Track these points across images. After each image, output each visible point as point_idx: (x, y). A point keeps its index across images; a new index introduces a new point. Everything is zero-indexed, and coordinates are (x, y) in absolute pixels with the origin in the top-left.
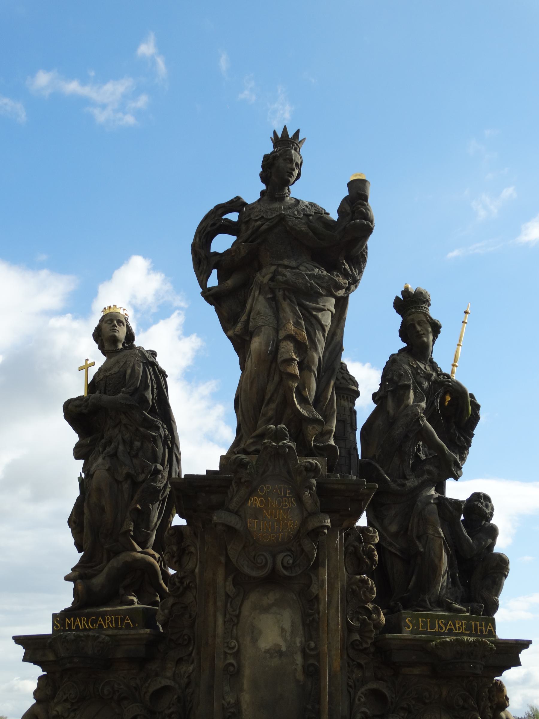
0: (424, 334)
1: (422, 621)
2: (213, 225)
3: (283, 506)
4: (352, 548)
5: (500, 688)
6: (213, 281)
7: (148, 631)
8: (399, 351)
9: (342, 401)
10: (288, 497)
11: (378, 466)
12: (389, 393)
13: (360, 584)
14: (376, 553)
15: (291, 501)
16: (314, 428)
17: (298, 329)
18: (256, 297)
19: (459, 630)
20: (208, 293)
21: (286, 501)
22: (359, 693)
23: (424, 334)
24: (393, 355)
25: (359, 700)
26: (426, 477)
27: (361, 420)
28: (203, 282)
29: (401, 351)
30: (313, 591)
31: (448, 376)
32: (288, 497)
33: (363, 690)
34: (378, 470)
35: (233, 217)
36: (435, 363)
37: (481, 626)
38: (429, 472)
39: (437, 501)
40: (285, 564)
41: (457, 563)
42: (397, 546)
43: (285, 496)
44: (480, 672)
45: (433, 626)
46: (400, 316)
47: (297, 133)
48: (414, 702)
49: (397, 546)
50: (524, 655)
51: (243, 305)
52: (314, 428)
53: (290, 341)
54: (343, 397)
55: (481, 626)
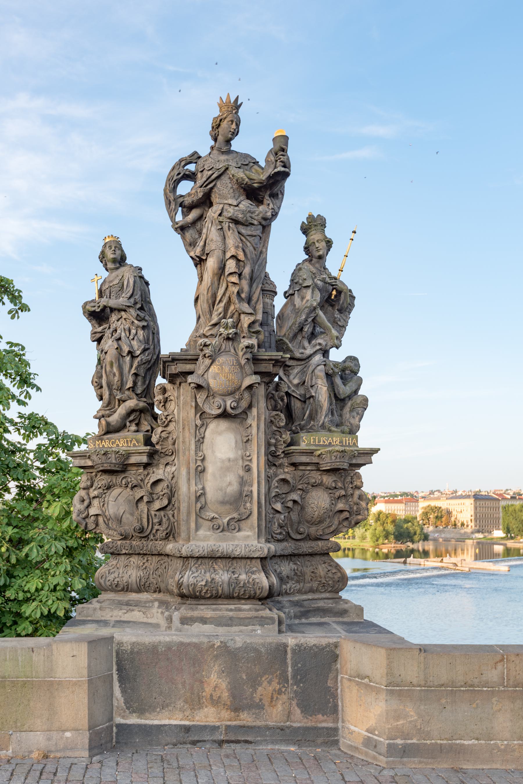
1: (313, 438)
2: (179, 174)
4: (271, 395)
5: (359, 477)
6: (179, 217)
7: (149, 447)
8: (303, 261)
11: (287, 342)
12: (296, 292)
14: (285, 398)
18: (209, 228)
19: (335, 442)
20: (177, 226)
22: (274, 481)
24: (299, 264)
25: (274, 485)
26: (318, 347)
27: (277, 312)
28: (172, 219)
29: (306, 260)
30: (249, 422)
31: (335, 278)
33: (277, 479)
34: (287, 344)
35: (192, 167)
36: (327, 269)
37: (349, 440)
38: (320, 344)
39: (324, 363)
40: (232, 406)
44: (346, 467)
45: (319, 442)
46: (304, 236)
48: (306, 486)
50: (374, 457)
51: (200, 233)
55: (349, 440)
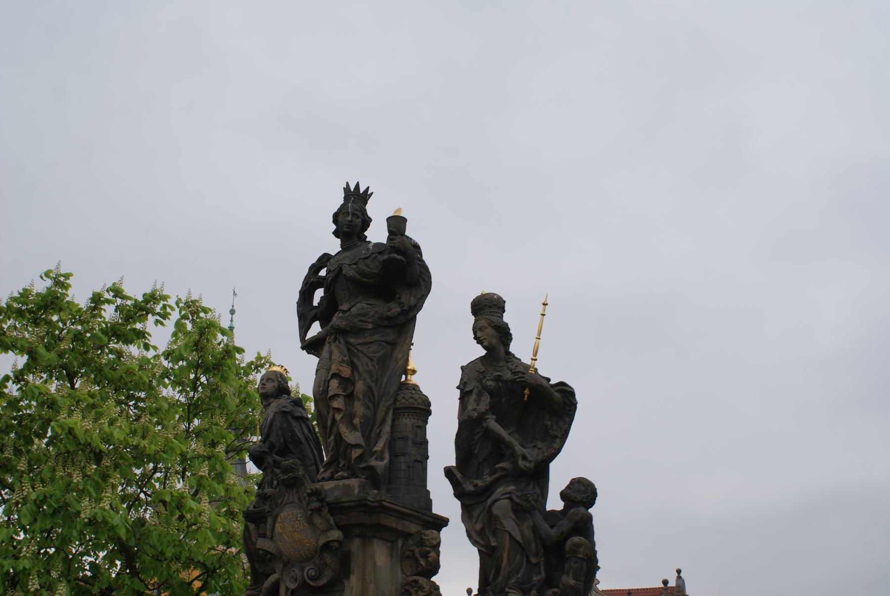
0: (485, 339)
3: (296, 529)
9: (404, 418)
10: (299, 521)
13: (414, 584)
15: (303, 523)
16: (355, 452)
17: (343, 366)
21: (298, 524)
23: (485, 339)
32: (299, 521)
38: (502, 469)
41: (542, 551)
42: (482, 542)
43: (297, 520)
47: (358, 185)
49: (482, 542)
52: (355, 452)
53: (336, 378)
54: (404, 415)
